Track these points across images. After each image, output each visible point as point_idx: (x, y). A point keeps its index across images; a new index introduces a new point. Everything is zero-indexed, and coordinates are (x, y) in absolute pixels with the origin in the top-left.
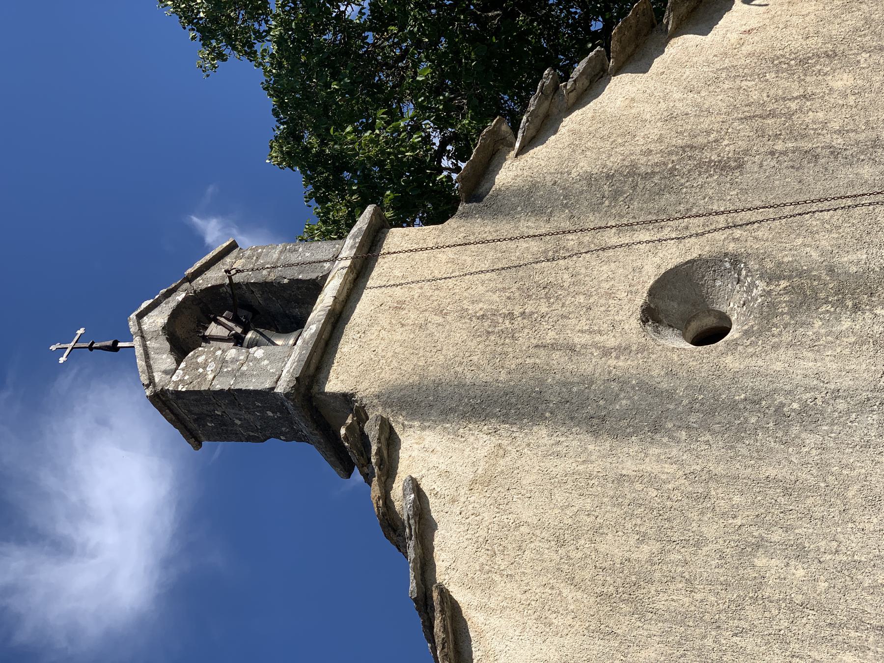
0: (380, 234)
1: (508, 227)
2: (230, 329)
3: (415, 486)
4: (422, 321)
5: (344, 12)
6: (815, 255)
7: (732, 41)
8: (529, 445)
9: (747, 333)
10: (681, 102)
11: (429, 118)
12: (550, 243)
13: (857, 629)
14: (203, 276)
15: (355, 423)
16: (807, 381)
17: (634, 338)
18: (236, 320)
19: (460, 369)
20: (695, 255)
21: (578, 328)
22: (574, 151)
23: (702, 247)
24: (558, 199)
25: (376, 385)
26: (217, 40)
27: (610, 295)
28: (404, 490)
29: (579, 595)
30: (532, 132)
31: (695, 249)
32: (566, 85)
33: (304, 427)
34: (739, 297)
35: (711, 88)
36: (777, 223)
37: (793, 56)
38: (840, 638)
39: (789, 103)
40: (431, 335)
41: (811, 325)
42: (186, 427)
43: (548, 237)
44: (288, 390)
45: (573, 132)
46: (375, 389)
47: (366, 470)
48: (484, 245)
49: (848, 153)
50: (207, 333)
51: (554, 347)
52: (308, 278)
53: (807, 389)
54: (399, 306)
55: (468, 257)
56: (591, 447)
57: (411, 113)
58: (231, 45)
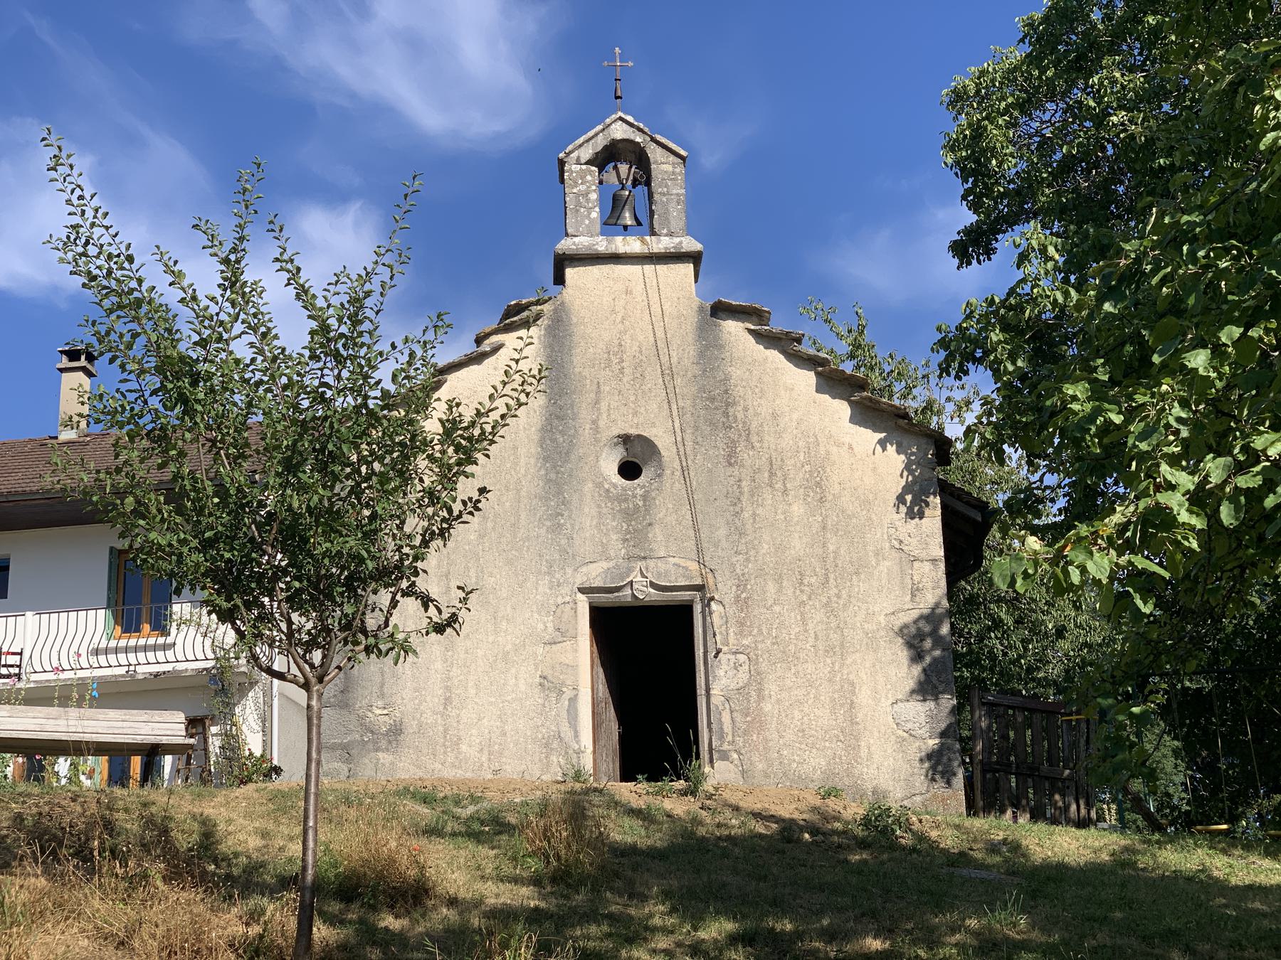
6: (661, 515)
53: (572, 525)
54: (628, 292)
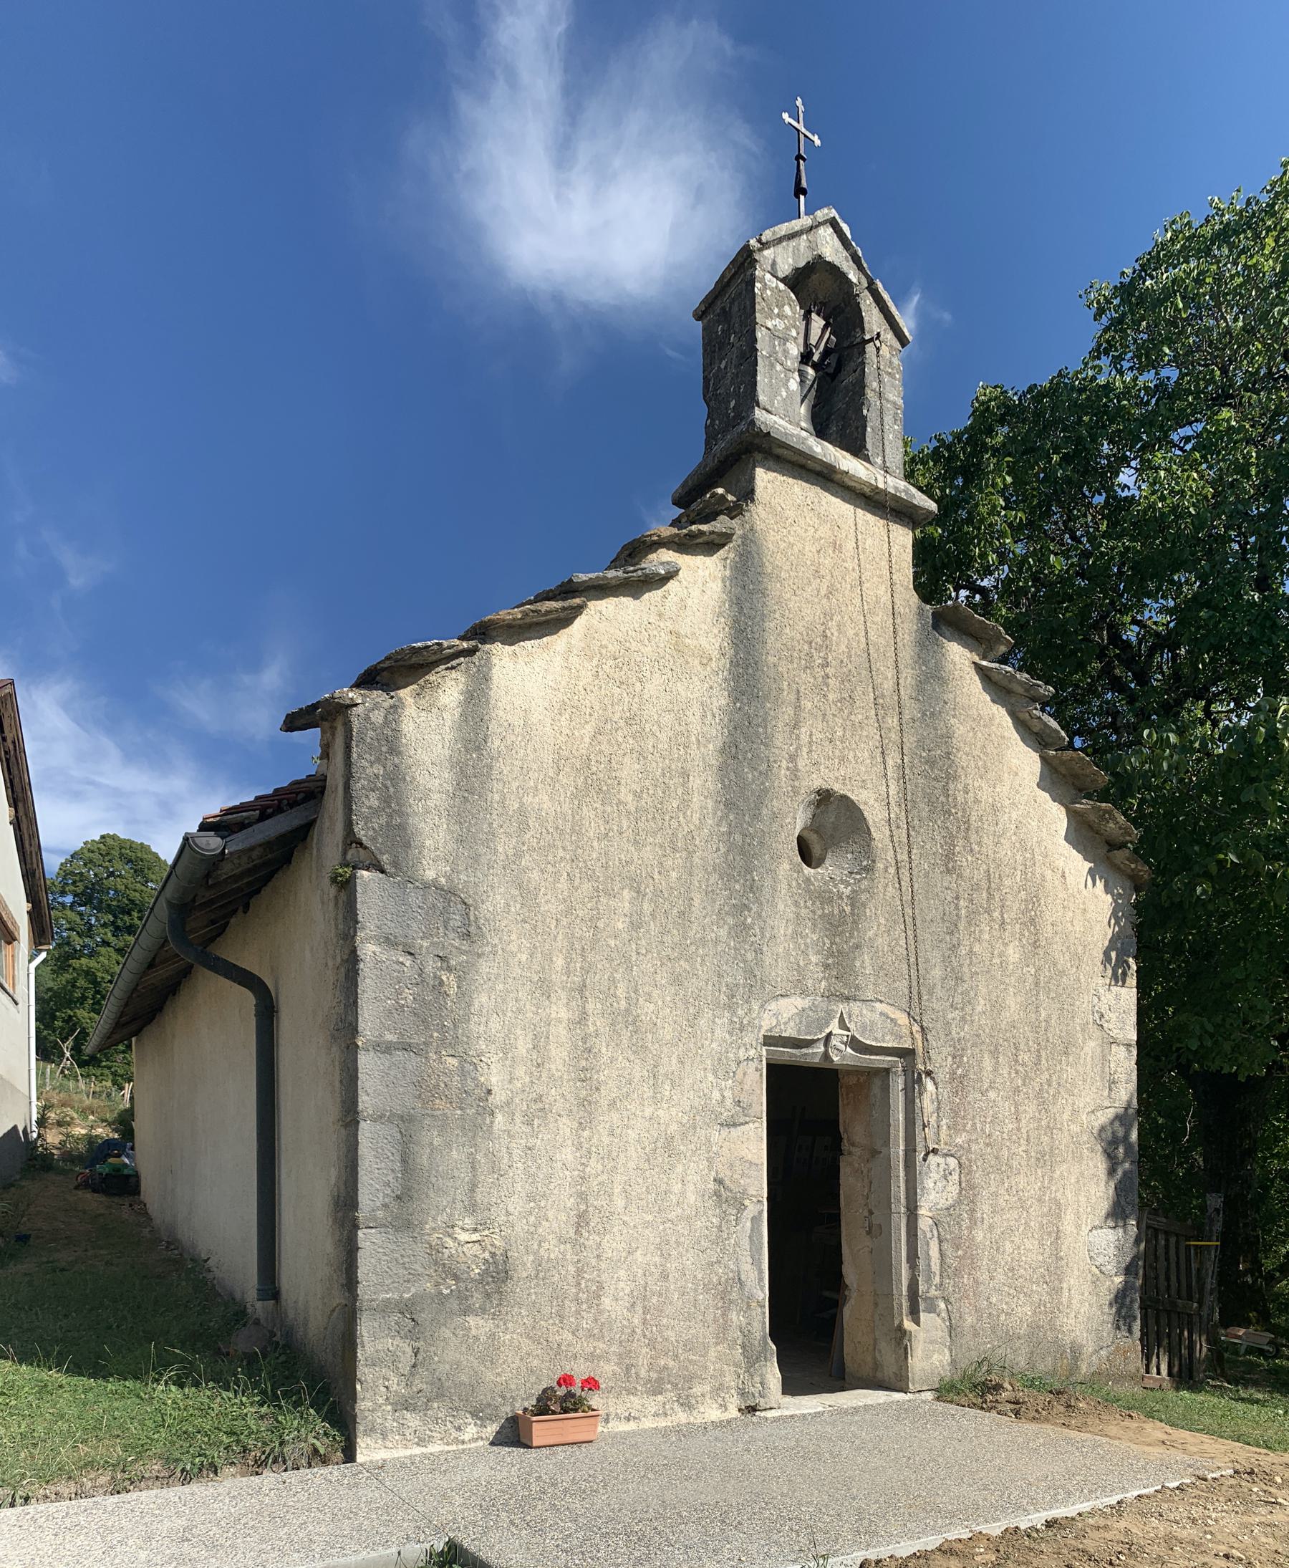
0: (907, 520)
1: (908, 657)
2: (817, 346)
3: (671, 575)
4: (822, 573)
5: (1129, 466)
6: (870, 934)
7: (1057, 862)
8: (711, 688)
9: (808, 880)
10: (1009, 818)
11: (1011, 570)
12: (891, 700)
13: (582, 968)
14: (874, 304)
15: (727, 505)
16: (769, 929)
17: (804, 783)
18: (827, 353)
19: (777, 616)
20: (874, 835)
21: (814, 731)
22: (974, 720)
23: (881, 841)
24: (931, 707)
25: (763, 526)
26: (1119, 306)
27: (843, 759)
28: (668, 563)
29: (587, 740)
30: (996, 677)
31: (880, 835)
32: (1036, 709)
33: (720, 447)
34: (837, 874)
35: (1017, 845)
36: (899, 903)
37: (1038, 913)
38: (574, 956)
39: (998, 910)
40: (809, 583)
41: (814, 932)
42: (716, 297)
43: (896, 698)
44: (757, 422)
45: (992, 719)
46: (759, 526)
47: (684, 520)
48: (892, 634)
49: (953, 958)
50: (814, 316)
51: (798, 708)
52: (867, 439)
53: (762, 929)
54: (837, 547)
55: (881, 618)
56: (711, 747)
57: (1018, 551)
58: (1111, 324)
